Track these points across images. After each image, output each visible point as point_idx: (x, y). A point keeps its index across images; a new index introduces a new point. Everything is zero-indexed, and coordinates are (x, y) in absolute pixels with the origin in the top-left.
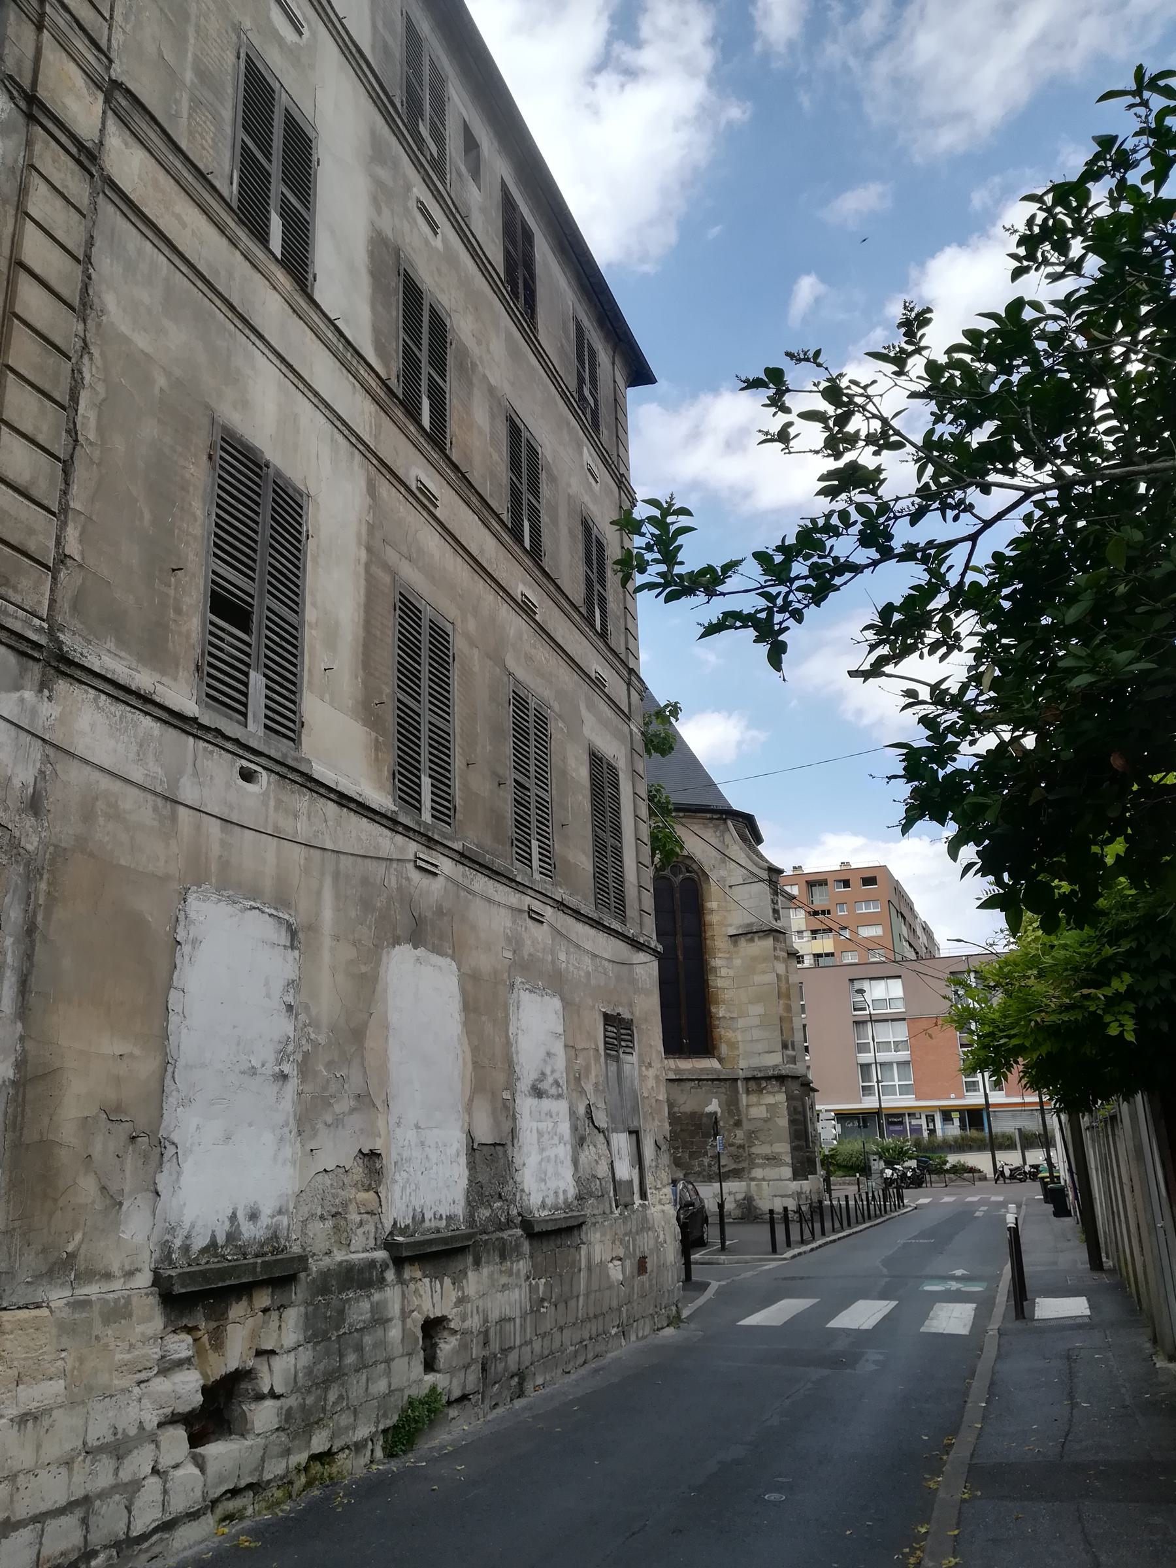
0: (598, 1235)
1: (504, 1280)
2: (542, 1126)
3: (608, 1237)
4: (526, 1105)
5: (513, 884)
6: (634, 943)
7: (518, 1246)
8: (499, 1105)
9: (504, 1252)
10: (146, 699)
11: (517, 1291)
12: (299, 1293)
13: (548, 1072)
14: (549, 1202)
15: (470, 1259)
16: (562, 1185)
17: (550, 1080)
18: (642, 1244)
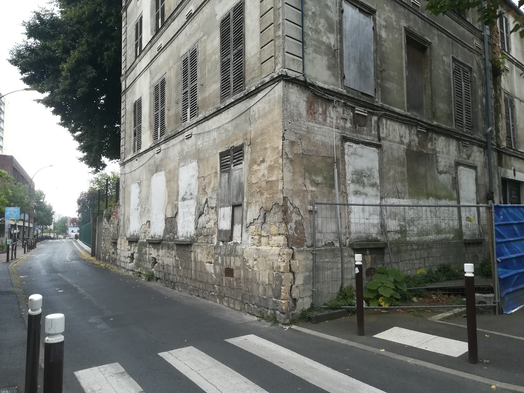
0: (199, 250)
1: (168, 254)
2: (185, 210)
3: (205, 252)
4: (180, 204)
5: (180, 133)
6: (249, 95)
7: (173, 247)
8: (174, 206)
9: (169, 247)
10: (128, 160)
11: (171, 259)
12: (138, 244)
13: (188, 191)
14: (184, 235)
15: (161, 247)
16: (190, 230)
17: (189, 194)
18: (228, 261)
